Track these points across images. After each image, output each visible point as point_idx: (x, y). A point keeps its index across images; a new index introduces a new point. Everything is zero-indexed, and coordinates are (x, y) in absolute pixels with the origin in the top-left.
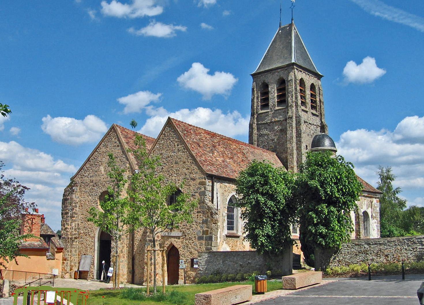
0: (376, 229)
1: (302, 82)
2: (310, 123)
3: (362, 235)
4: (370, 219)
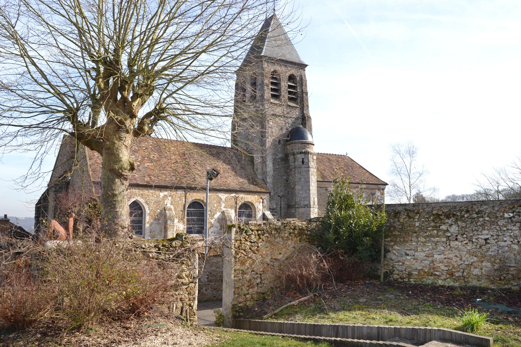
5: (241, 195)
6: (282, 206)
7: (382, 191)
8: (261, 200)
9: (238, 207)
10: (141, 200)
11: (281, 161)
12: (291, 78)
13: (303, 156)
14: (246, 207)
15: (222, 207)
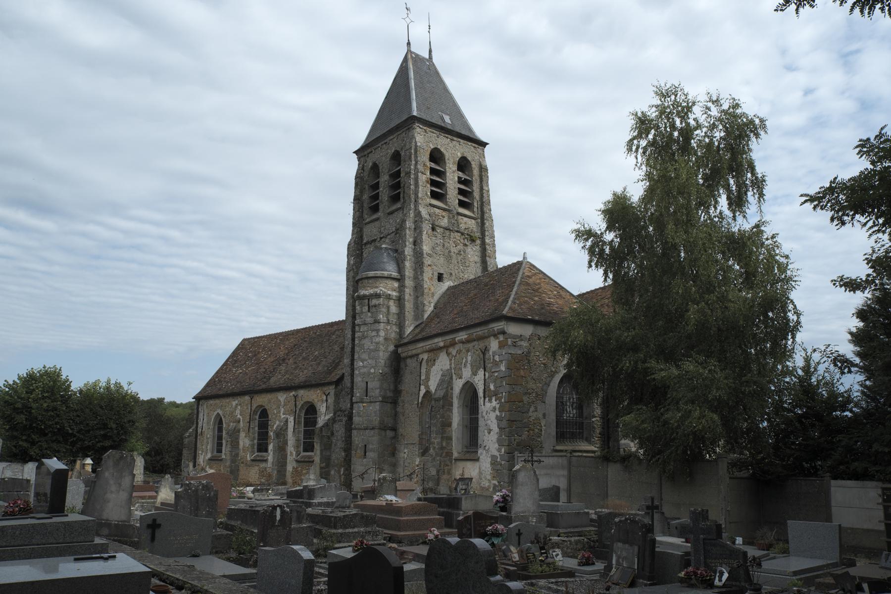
0: (495, 428)
2: (381, 238)
3: (434, 448)
4: (481, 401)
5: (301, 392)
7: (501, 338)
8: (325, 398)
10: (221, 413)
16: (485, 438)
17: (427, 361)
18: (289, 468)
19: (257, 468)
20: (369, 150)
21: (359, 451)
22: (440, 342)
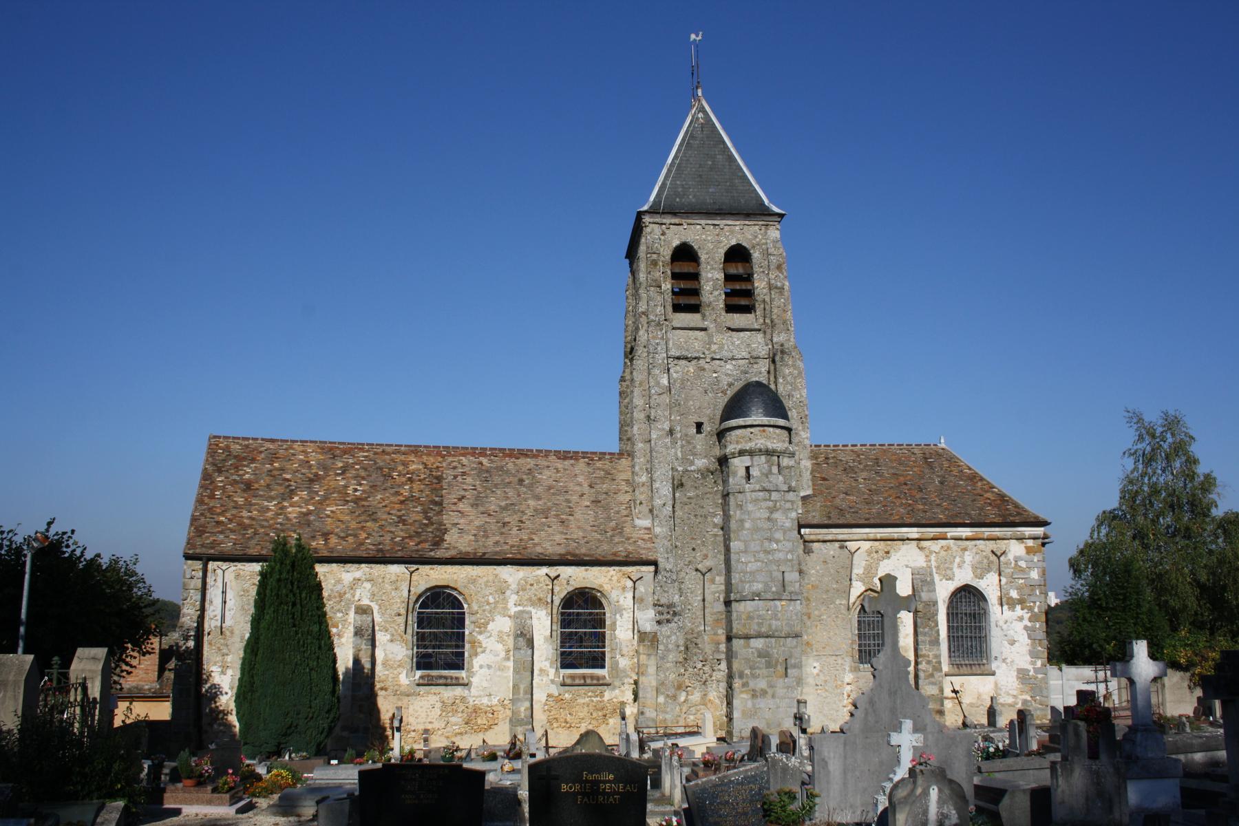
0: (1023, 640)
1: (684, 253)
2: (713, 359)
5: (566, 571)
6: (709, 598)
7: (1030, 543)
9: (557, 601)
11: (704, 477)
12: (737, 254)
13: (746, 461)
14: (586, 602)
15: (511, 604)
16: (1004, 650)
17: (869, 553)
18: (540, 696)
19: (433, 699)
20: (677, 221)
21: (779, 667)
22: (914, 532)
